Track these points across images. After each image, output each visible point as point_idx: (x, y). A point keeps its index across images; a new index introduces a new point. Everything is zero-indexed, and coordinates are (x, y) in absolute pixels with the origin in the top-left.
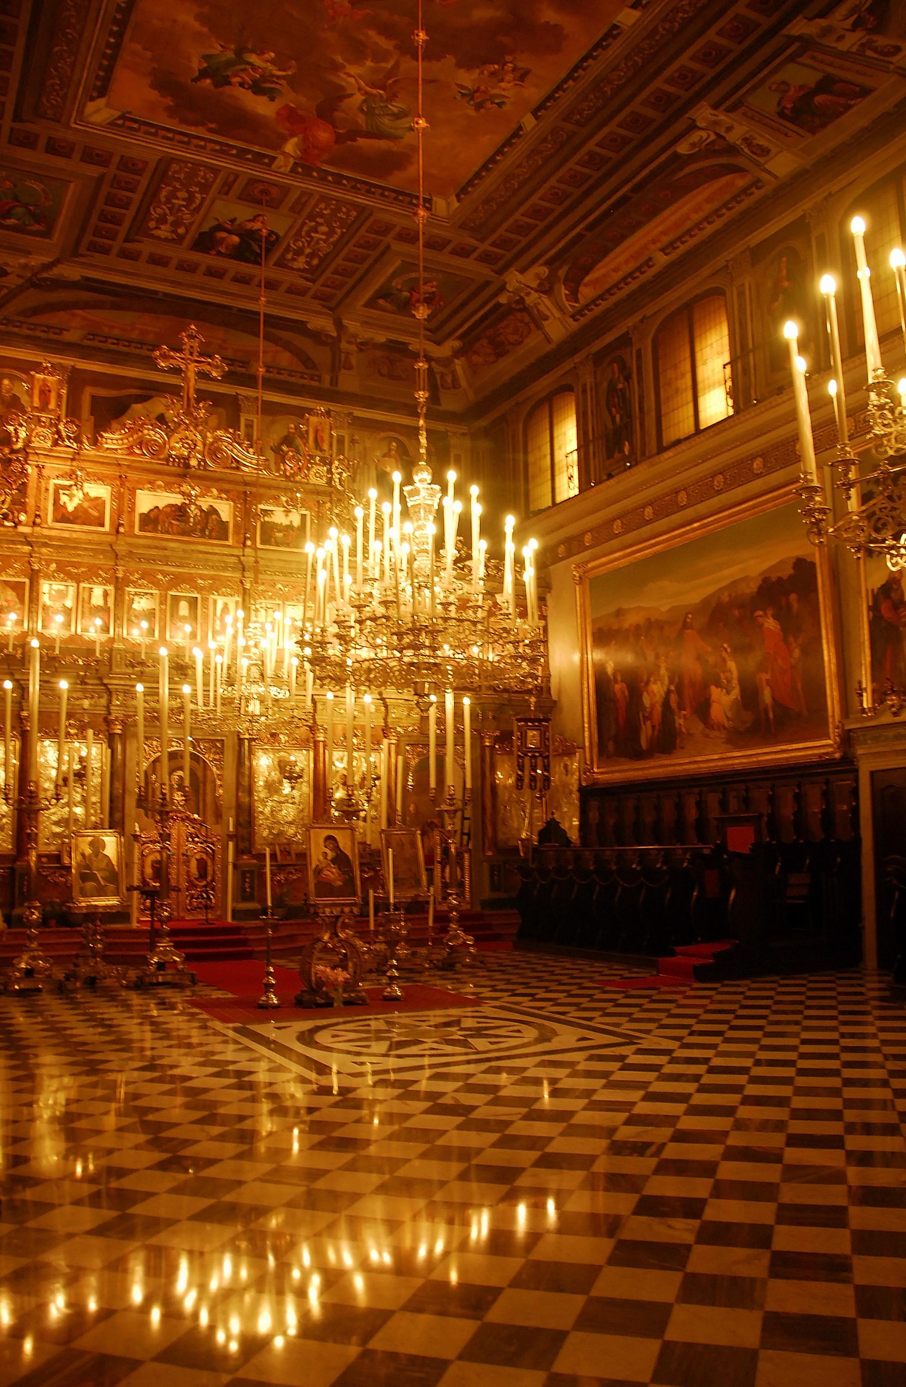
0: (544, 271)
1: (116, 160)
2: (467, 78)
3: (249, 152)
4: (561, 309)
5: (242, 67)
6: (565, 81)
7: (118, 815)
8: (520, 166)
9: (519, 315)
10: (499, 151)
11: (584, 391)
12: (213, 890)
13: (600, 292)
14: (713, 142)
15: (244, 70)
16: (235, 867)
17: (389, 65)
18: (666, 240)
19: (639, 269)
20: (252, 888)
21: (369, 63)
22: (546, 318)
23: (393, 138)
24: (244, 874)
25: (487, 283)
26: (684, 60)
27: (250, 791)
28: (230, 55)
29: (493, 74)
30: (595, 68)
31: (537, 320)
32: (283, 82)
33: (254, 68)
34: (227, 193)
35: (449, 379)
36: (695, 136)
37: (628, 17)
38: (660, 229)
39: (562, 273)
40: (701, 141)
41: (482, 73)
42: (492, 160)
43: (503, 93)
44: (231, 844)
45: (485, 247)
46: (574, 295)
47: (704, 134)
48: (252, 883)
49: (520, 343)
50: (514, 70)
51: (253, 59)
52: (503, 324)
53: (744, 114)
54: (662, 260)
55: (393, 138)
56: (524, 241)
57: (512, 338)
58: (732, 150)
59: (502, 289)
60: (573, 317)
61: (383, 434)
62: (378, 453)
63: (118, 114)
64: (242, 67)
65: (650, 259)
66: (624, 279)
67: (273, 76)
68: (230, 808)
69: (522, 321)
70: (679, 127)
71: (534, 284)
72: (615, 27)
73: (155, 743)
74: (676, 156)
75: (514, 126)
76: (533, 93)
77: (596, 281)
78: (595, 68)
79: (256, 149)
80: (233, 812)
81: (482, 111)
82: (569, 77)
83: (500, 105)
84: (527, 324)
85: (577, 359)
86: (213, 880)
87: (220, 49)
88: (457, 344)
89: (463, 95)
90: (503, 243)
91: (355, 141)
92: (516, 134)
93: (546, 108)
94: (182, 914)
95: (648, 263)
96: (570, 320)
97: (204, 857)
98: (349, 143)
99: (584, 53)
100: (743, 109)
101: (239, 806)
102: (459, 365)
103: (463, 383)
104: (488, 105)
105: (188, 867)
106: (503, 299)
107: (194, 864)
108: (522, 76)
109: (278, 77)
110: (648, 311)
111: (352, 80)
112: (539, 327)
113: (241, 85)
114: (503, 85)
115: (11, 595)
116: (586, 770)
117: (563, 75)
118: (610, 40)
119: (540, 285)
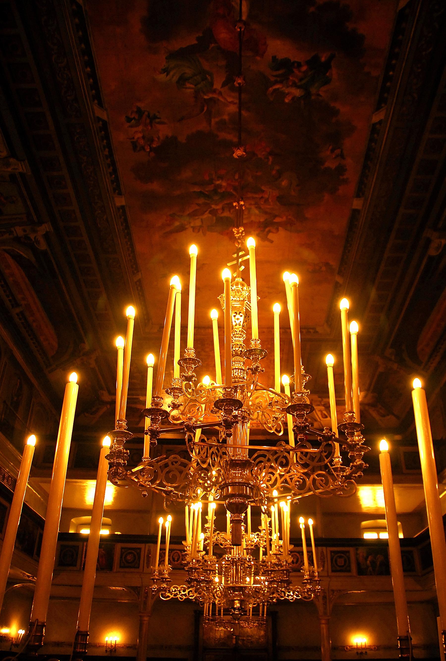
2: (164, 131)
5: (303, 82)
6: (110, 151)
10: (93, 75)
15: (301, 80)
17: (213, 121)
21: (226, 117)
23: (172, 56)
28: (313, 90)
29: (152, 141)
32: (273, 79)
33: (295, 85)
42: (90, 63)
43: (134, 129)
50: (143, 148)
51: (297, 92)
55: (172, 56)
64: (303, 82)
67: (281, 82)
72: (120, 194)
81: (135, 110)
83: (129, 120)
87: (321, 93)
89: (155, 117)
91: (198, 39)
92: (98, 97)
98: (201, 35)
108: (135, 146)
109: (276, 82)
111: (230, 100)
113: (299, 65)
114: (140, 135)
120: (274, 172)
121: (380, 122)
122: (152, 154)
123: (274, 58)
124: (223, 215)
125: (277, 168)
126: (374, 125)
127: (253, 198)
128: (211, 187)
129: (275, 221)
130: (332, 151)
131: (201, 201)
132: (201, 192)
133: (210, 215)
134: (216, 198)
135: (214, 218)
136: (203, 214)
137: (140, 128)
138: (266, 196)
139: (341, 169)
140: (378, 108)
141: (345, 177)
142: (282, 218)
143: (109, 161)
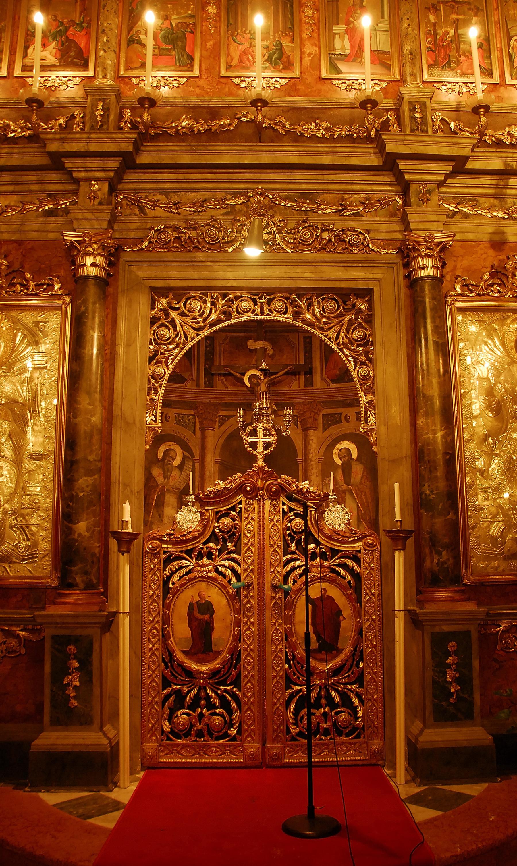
12: (360, 680)
16: (414, 620)
20: (464, 681)
24: (439, 642)
27: (448, 417)
44: (399, 558)
48: (464, 665)
68: (394, 462)
73: (196, 304)
80: (405, 471)
86: (358, 654)
94: (274, 748)
97: (334, 592)
101: (420, 455)
105: (289, 620)
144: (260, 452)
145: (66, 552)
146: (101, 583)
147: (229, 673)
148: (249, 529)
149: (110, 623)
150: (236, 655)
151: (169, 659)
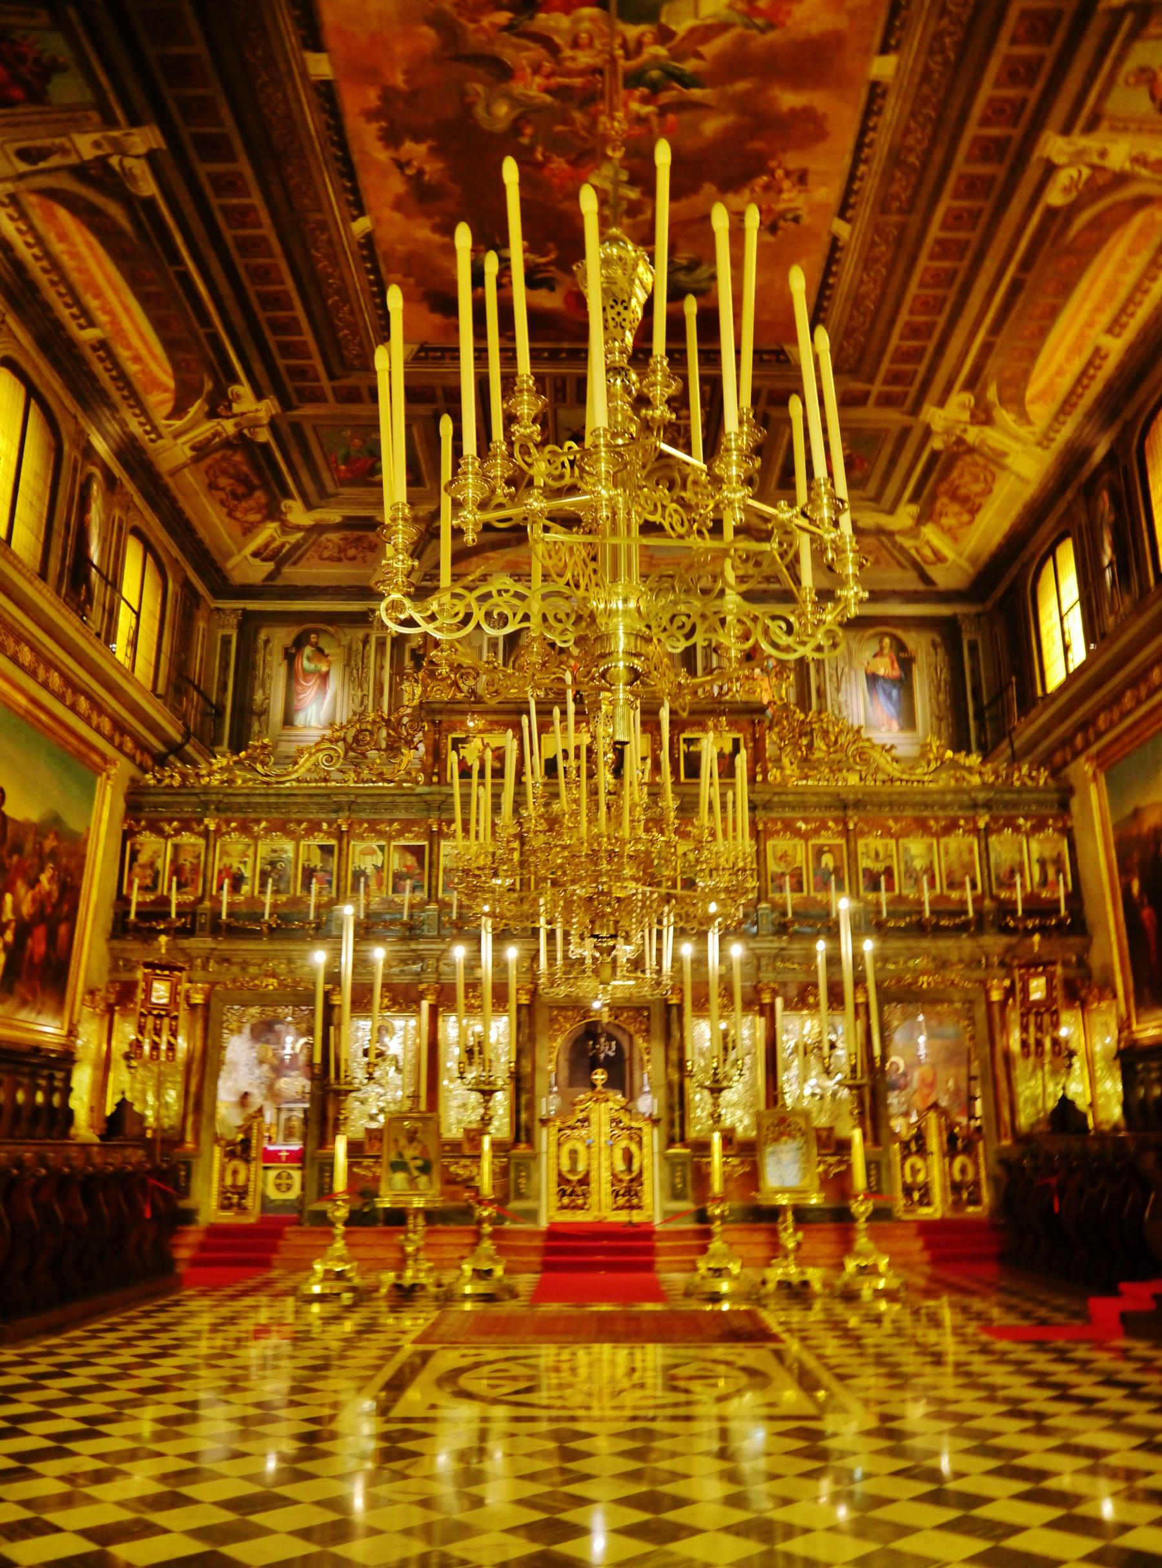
0: (968, 398)
1: (439, 393)
3: (562, 350)
4: (1017, 438)
7: (524, 1099)
8: (861, 282)
9: (968, 459)
11: (1081, 535)
13: (1054, 406)
14: (1091, 179)
18: (1105, 319)
19: (1090, 363)
22: (1005, 454)
25: (906, 432)
26: (986, 91)
29: (767, 188)
30: (882, 141)
31: (996, 460)
34: (564, 399)
35: (927, 552)
36: (1063, 178)
37: (884, 67)
38: (1088, 306)
39: (992, 393)
40: (1074, 183)
41: (753, 191)
45: (877, 388)
46: (1023, 417)
47: (1073, 172)
48: (684, 1177)
49: (990, 491)
50: (788, 174)
52: (955, 473)
53: (1112, 128)
54: (1116, 347)
56: (922, 369)
57: (977, 488)
58: (1121, 179)
59: (928, 433)
60: (1039, 444)
61: (871, 632)
62: (867, 655)
63: (416, 347)
65: (1097, 351)
66: (1078, 381)
67: (538, 265)
69: (976, 464)
70: (1032, 174)
71: (966, 416)
72: (875, 85)
74: (1051, 212)
75: (826, 239)
76: (827, 193)
77: (1041, 396)
78: (882, 141)
79: (566, 345)
82: (856, 161)
83: (796, 220)
84: (985, 467)
85: (1069, 495)
88: (914, 509)
90: (895, 378)
93: (853, 207)
95: (1098, 353)
96: (1038, 450)
99: (856, 126)
100: (1105, 125)
102: (929, 532)
103: (947, 551)
104: (782, 223)
106: (937, 443)
107: (618, 1154)
108: (802, 178)
109: (546, 264)
110: (1128, 414)
112: (1004, 468)
114: (785, 196)
115: (410, 860)
116: (1124, 1025)
117: (847, 160)
118: (879, 101)
119: (973, 416)
120: (529, 130)
121: (354, 218)
122: (773, 164)
123: (552, 289)
124: (642, 28)
125: (525, 141)
126: (362, 213)
127: (569, 74)
128: (665, 97)
129: (509, 15)
130: (421, 172)
131: (690, 65)
132: (687, 86)
133: (673, 27)
134: (655, 74)
135: (663, 20)
136: (692, 31)
137: (781, 206)
138: (538, 80)
139: (391, 139)
140: (369, 237)
141: (375, 126)
142: (493, 25)
143: (867, 151)
144: (599, 1083)
145: (517, 1127)
146: (530, 1141)
147: (585, 1181)
148: (594, 1117)
149: (535, 1157)
150: (588, 1174)
151: (560, 1174)
